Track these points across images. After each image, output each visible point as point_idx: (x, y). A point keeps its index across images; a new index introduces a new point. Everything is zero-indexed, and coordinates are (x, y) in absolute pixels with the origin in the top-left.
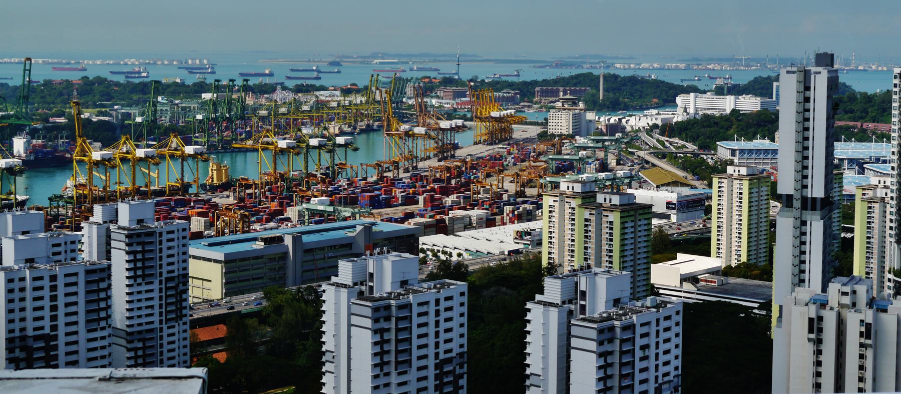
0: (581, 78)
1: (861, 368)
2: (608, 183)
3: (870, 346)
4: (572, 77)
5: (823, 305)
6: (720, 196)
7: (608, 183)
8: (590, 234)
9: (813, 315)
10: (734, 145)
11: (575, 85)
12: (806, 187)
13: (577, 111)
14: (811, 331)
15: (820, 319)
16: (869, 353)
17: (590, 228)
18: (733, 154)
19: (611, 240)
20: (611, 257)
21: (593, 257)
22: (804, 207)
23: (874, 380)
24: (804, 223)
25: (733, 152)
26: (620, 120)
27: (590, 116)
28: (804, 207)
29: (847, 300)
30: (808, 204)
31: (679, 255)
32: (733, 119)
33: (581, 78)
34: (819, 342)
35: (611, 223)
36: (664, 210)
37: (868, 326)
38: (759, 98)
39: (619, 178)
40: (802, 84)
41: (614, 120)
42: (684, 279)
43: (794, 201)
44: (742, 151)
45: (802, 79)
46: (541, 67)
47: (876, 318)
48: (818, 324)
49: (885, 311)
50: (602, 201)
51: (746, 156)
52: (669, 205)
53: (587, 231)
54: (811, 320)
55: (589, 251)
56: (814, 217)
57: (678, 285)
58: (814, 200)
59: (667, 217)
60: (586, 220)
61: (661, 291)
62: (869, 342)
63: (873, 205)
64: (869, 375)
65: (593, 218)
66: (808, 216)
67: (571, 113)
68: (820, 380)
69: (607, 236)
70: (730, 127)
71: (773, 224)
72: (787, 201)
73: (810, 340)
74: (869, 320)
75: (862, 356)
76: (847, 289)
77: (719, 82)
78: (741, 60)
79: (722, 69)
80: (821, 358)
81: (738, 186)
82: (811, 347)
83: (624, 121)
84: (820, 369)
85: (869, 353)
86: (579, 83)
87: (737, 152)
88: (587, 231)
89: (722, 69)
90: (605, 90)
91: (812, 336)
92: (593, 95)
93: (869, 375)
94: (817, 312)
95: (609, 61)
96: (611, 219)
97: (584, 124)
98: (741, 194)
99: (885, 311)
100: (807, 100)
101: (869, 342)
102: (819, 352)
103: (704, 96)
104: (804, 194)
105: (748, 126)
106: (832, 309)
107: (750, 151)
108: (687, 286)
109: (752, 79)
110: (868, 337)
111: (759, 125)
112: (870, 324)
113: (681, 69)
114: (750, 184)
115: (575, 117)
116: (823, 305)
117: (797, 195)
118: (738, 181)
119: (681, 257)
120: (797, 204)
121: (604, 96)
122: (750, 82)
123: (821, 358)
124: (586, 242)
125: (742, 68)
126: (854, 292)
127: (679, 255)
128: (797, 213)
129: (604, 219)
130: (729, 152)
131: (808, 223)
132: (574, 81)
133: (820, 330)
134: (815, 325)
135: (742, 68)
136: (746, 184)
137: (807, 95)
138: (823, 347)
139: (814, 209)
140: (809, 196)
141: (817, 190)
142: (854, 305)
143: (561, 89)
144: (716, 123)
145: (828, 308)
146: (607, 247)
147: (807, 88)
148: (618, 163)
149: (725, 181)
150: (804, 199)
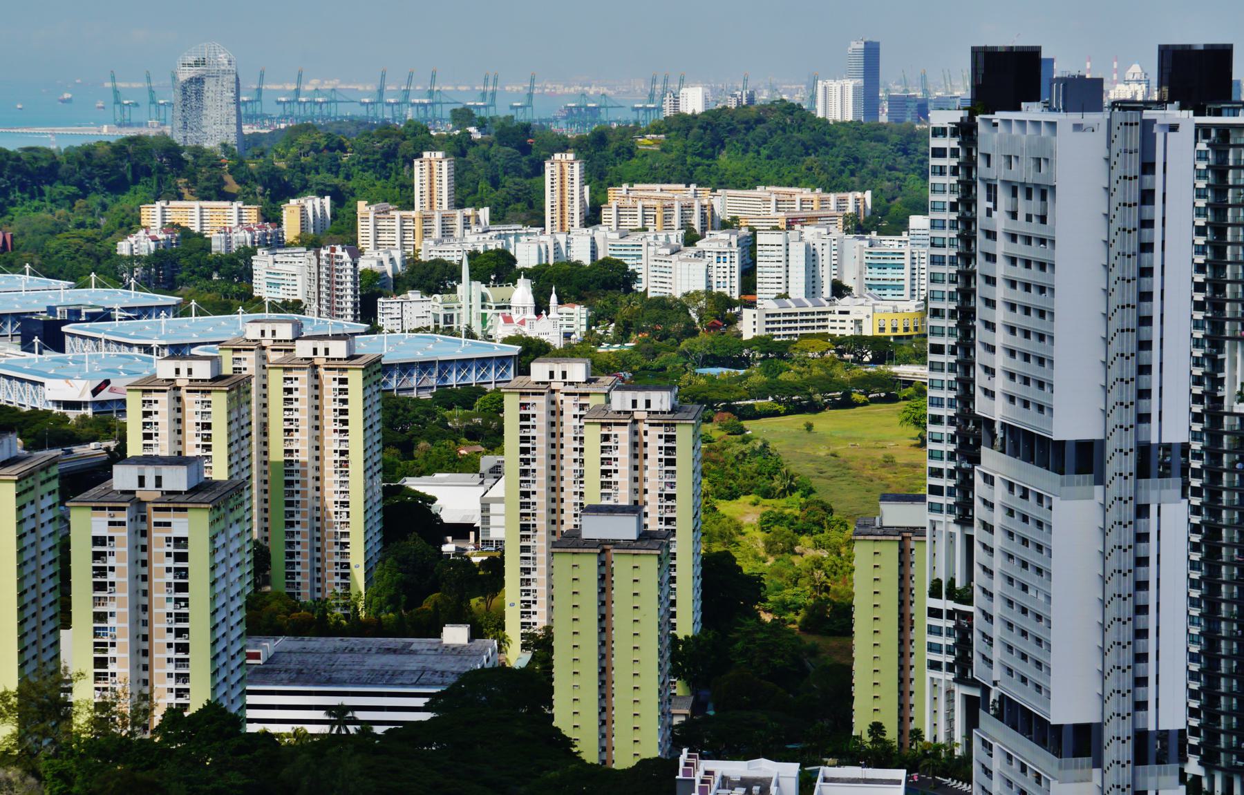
6: (147, 436)
8: (111, 577)
17: (111, 562)
19: (182, 587)
20: (180, 633)
21: (124, 640)
24: (1142, 511)
35: (180, 541)
45: (1135, 141)
50: (133, 485)
53: (100, 571)
55: (111, 622)
56: (1165, 493)
60: (98, 541)
63: (615, 430)
65: (122, 534)
69: (170, 578)
71: (169, 493)
72: (1084, 459)
81: (199, 408)
88: (100, 571)
96: (178, 530)
98: (208, 426)
100: (1147, 197)
114: (230, 400)
118: (198, 397)
120: (1119, 464)
124: (97, 601)
128: (1128, 488)
129: (158, 534)
136: (219, 401)
137: (1147, 186)
141: (1175, 424)
146: (170, 607)
147: (1148, 167)
149: (163, 398)
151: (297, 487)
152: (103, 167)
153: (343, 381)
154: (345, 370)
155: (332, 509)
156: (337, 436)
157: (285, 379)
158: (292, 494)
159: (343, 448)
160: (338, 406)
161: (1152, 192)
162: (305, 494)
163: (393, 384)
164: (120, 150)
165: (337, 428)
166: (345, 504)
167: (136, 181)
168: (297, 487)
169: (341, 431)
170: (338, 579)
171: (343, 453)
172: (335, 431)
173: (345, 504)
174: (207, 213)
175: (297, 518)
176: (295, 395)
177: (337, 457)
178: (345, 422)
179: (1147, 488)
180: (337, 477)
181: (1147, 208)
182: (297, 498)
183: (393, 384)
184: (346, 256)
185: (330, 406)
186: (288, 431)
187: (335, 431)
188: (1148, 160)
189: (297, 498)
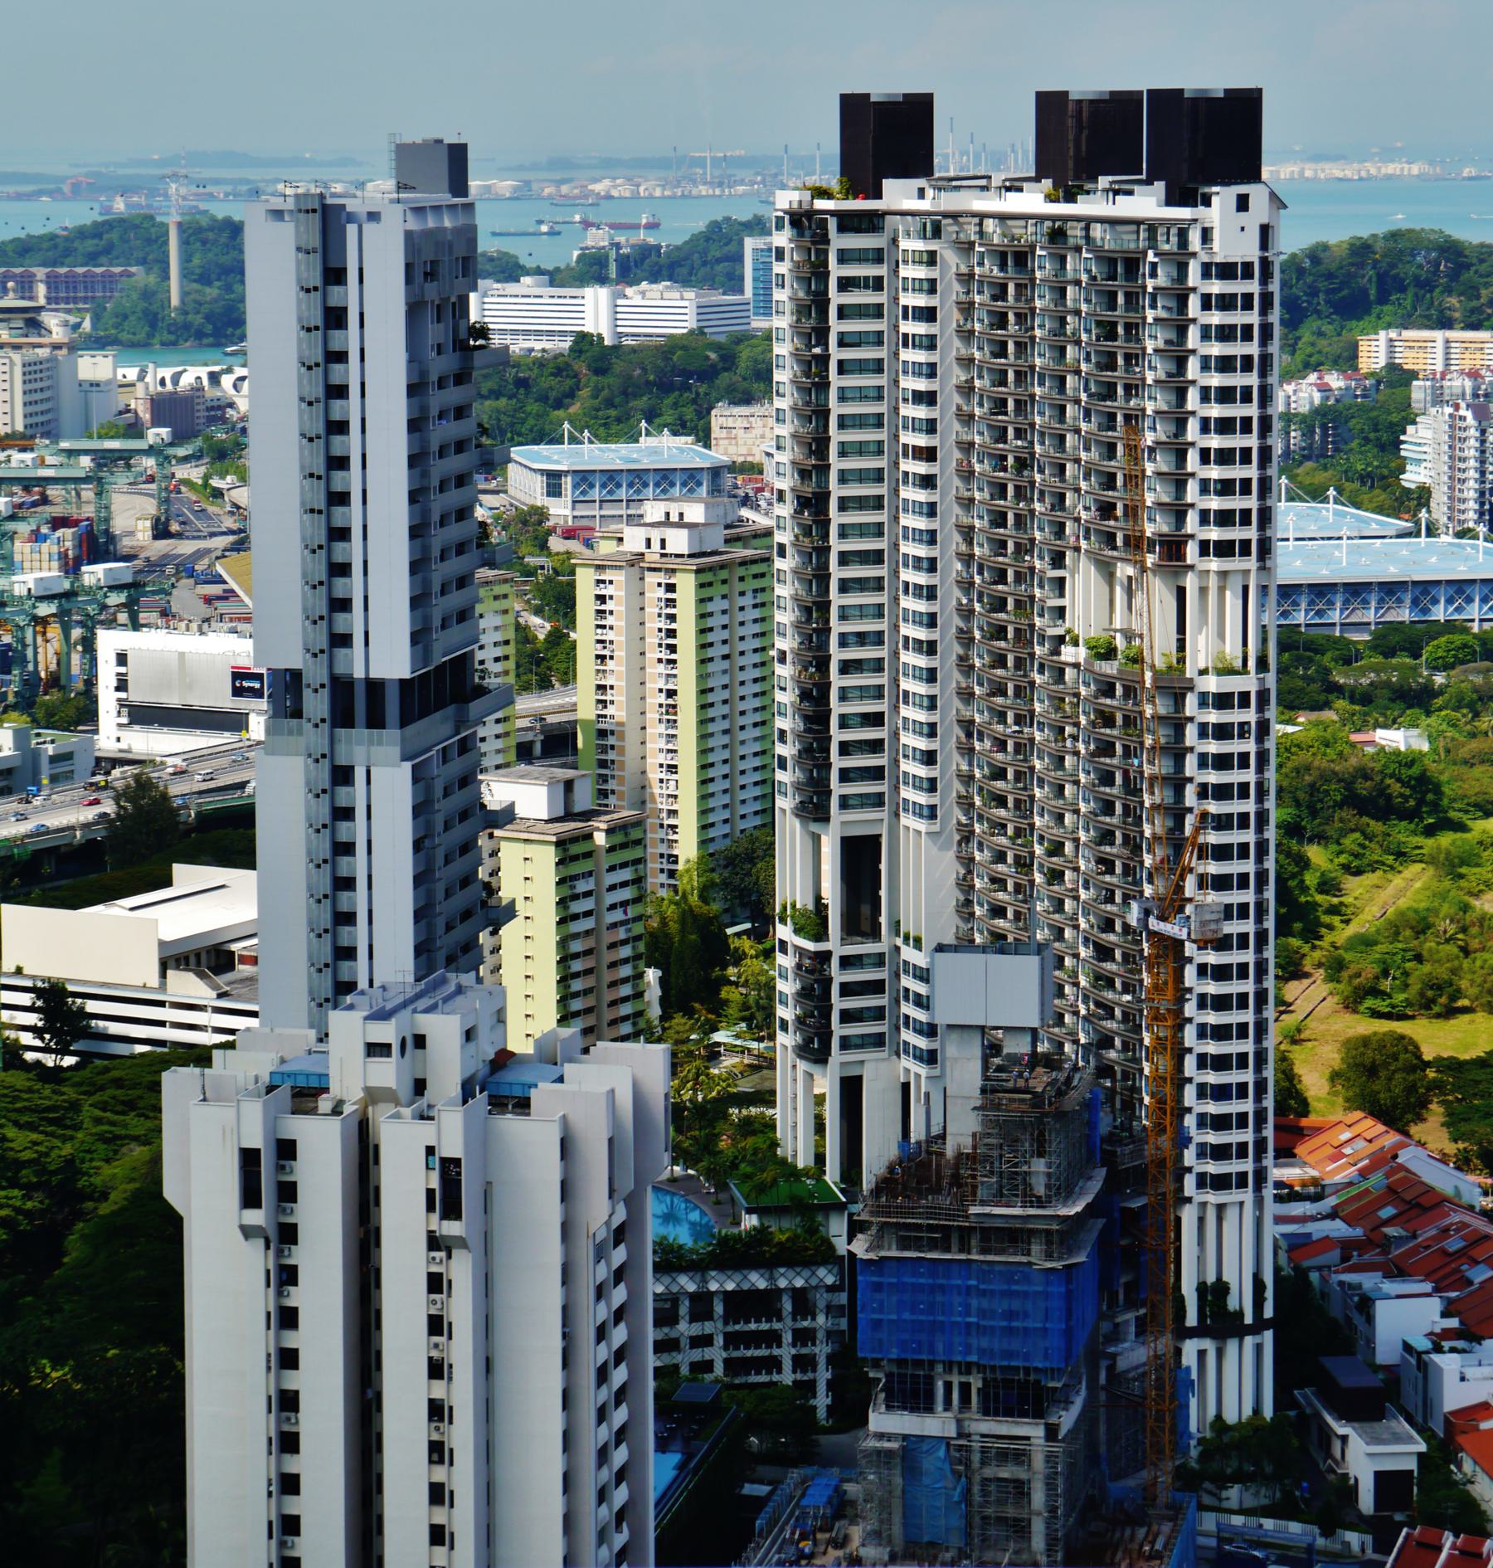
0: (114, 236)
1: (436, 1325)
2: (44, 609)
3: (461, 1242)
4: (82, 233)
5: (306, 1095)
7: (44, 609)
9: (255, 1139)
10: (557, 456)
11: (92, 258)
12: (344, 640)
13: (43, 353)
14: (250, 1198)
15: (286, 1150)
16: (461, 1271)
18: (554, 490)
22: (342, 716)
23: (487, 1366)
24: (343, 775)
25: (553, 481)
26: (214, 378)
27: (94, 366)
28: (342, 716)
29: (386, 1073)
30: (356, 704)
31: (178, 869)
32: (581, 367)
33: (114, 236)
34: (288, 1235)
36: (224, 700)
37: (450, 1169)
38: (690, 294)
39: (89, 591)
40: (317, 259)
41: (193, 375)
42: (175, 958)
43: (307, 694)
44: (584, 478)
45: (315, 241)
46: (19, 197)
47: (481, 1140)
48: (281, 1169)
49: (523, 1105)
51: (596, 494)
52: (242, 683)
54: (249, 1159)
56: (376, 751)
57: (154, 981)
58: (375, 687)
59: (236, 722)
61: (92, 1007)
62: (452, 1228)
64: (462, 1351)
66: (358, 746)
67: (17, 357)
68: (292, 1380)
70: (571, 394)
73: (248, 1232)
74: (452, 1148)
75: (436, 1283)
76: (385, 1032)
77: (597, 239)
78: (701, 162)
79: (636, 196)
80: (296, 1297)
82: (255, 1260)
83: (227, 381)
84: (291, 1340)
85: (461, 1271)
86: (108, 250)
87: (567, 483)
89: (636, 196)
90: (185, 274)
91: (256, 1217)
92: (147, 294)
93: (462, 1351)
94: (271, 1123)
95: (253, 174)
97: (69, 404)
99: (523, 1105)
100: (335, 318)
101: (452, 1228)
102: (288, 1276)
103: (511, 288)
104: (340, 669)
105: (629, 391)
106: (336, 1111)
107: (611, 477)
108: (187, 985)
109: (700, 225)
110: (452, 1210)
111: (664, 386)
112: (457, 1162)
113: (499, 198)
115: (34, 373)
116: (306, 1095)
117: (316, 673)
119: (185, 875)
120: (317, 704)
121: (184, 294)
122: (695, 238)
123: (296, 1297)
125: (703, 190)
126: (420, 1041)
127: (178, 869)
128: (318, 739)
130: (539, 483)
131: (360, 774)
132: (90, 245)
133: (287, 1193)
134: (265, 1177)
135: (703, 190)
137: (333, 302)
138: (299, 1256)
139: (376, 721)
140: (359, 673)
142: (420, 1087)
143: (41, 272)
144: (522, 383)
145: (325, 1104)
147: (335, 275)
148: (161, 531)
150: (341, 687)
151: (611, 740)
152: (1330, 276)
153: (671, 588)
154: (674, 571)
155: (654, 775)
156: (661, 668)
157: (599, 582)
158: (604, 749)
159: (671, 686)
160: (664, 624)
161: (344, 310)
162: (622, 752)
163: (1335, 616)
164: (1361, 250)
165: (663, 656)
166: (672, 769)
167: (1383, 299)
168: (611, 740)
169: (670, 662)
170: (663, 878)
171: (671, 693)
172: (660, 661)
173: (672, 769)
174: (1456, 349)
175: (611, 785)
176: (608, 607)
177: (662, 698)
178: (672, 648)
179: (349, 742)
180: (662, 729)
181: (336, 334)
182: (611, 756)
183: (1335, 616)
184: (1470, 420)
185: (654, 624)
186: (602, 658)
187: (660, 661)
188: (333, 264)
189: (611, 756)
